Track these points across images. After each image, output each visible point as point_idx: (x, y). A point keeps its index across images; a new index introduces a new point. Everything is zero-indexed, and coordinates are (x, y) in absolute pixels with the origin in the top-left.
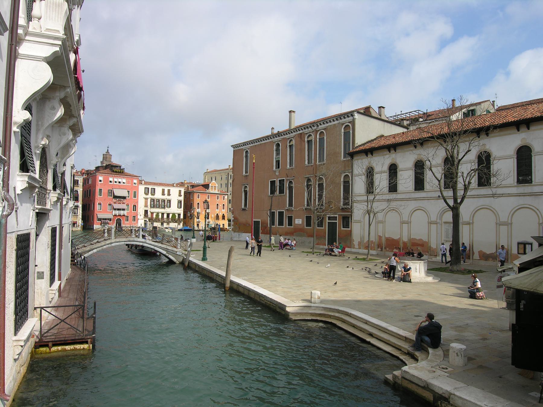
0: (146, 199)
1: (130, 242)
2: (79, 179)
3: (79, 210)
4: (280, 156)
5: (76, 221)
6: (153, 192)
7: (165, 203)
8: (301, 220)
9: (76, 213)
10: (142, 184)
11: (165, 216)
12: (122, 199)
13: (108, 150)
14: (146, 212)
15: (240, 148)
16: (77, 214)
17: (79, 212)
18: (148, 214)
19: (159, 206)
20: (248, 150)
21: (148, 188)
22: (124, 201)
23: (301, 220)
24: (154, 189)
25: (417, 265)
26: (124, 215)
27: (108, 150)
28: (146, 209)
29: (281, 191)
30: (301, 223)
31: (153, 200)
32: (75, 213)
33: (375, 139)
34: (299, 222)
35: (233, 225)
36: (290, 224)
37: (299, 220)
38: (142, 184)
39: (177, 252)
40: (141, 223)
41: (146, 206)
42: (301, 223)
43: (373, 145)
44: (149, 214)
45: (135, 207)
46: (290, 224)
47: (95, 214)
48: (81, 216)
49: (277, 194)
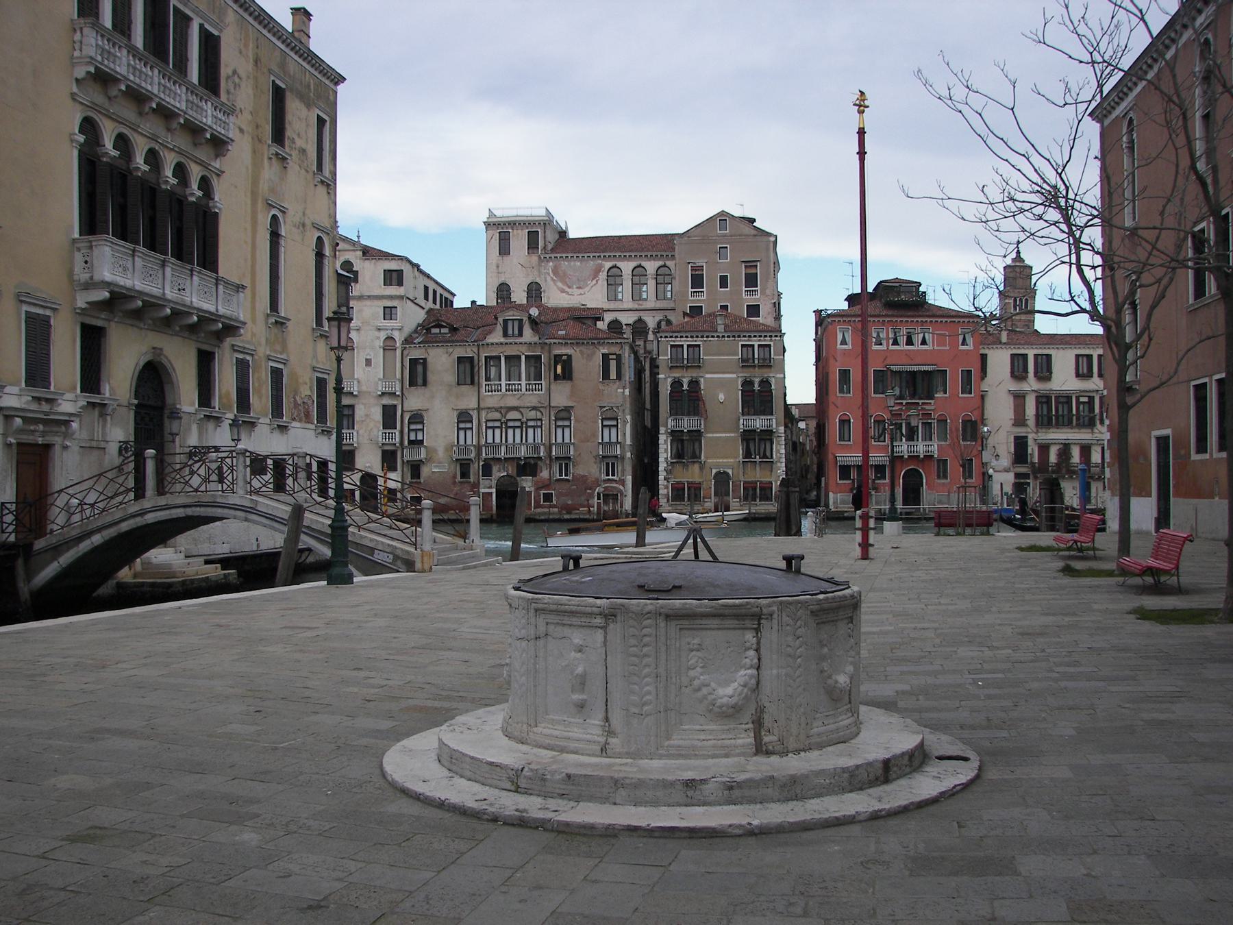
0: (1019, 398)
1: (202, 509)
2: (772, 343)
3: (778, 443)
5: (768, 480)
6: (1045, 368)
7: (1050, 409)
9: (768, 454)
10: (1001, 343)
11: (1076, 453)
12: (921, 402)
14: (1021, 444)
15: (1114, 116)
16: (772, 458)
17: (778, 451)
18: (1030, 451)
19: (1050, 419)
21: (1025, 356)
22: (927, 407)
24: (1049, 357)
25: (577, 638)
26: (929, 457)
27: (1018, 252)
28: (1021, 431)
31: (1043, 400)
32: (765, 456)
38: (1001, 343)
40: (1003, 480)
41: (1020, 420)
44: (1033, 449)
45: (972, 429)
47: (830, 457)
48: (784, 465)
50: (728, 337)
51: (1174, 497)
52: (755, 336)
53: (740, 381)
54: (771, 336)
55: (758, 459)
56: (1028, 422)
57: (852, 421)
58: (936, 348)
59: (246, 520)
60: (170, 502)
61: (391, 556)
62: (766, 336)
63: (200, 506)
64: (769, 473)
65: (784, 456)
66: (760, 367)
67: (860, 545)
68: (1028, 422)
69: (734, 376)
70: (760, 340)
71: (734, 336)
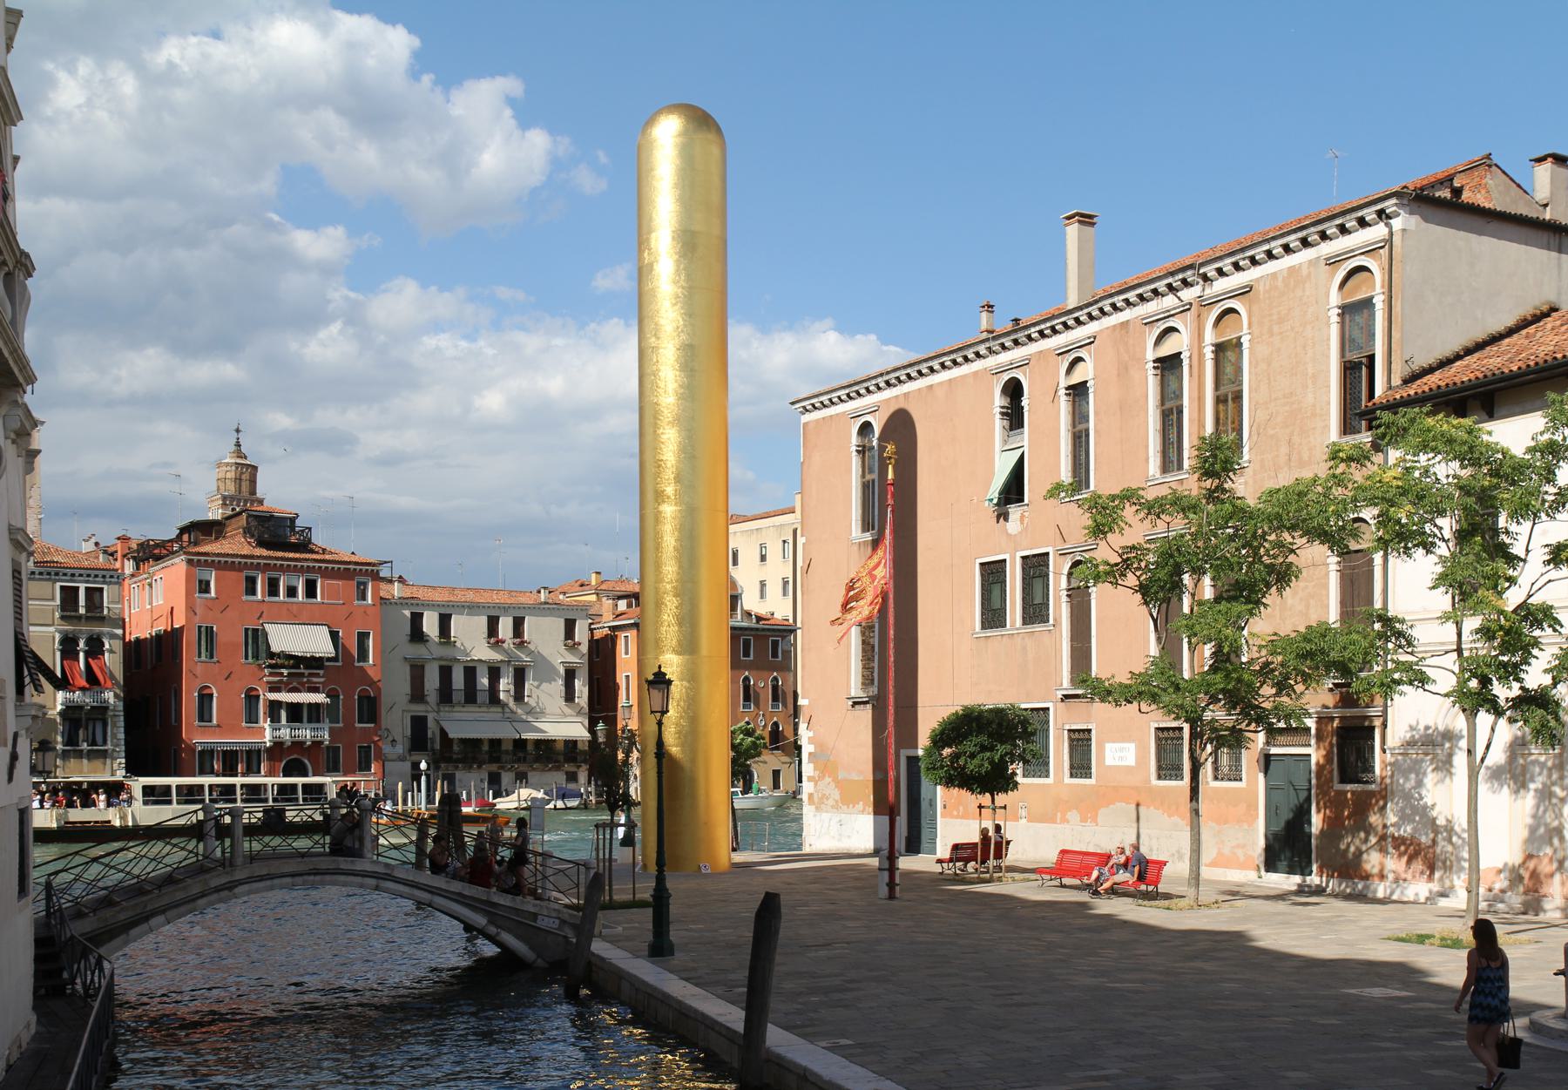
4: (1026, 443)
8: (1132, 746)
13: (238, 445)
14: (419, 724)
18: (430, 735)
20: (869, 418)
22: (315, 680)
23: (1132, 746)
28: (419, 709)
29: (1035, 612)
30: (1130, 760)
33: (1511, 332)
34: (1121, 758)
35: (810, 779)
36: (1081, 766)
37: (1122, 750)
39: (535, 916)
41: (418, 695)
42: (1130, 760)
43: (1495, 361)
46: (1081, 766)
49: (1013, 624)
50: (41, 574)
51: (942, 816)
52: (81, 575)
53: (58, 637)
54: (104, 577)
55: (85, 746)
56: (428, 699)
57: (215, 695)
58: (326, 601)
59: (377, 888)
60: (273, 871)
61: (557, 921)
62: (96, 576)
63: (315, 874)
64: (101, 766)
65: (123, 742)
66: (88, 618)
67: (887, 885)
68: (429, 699)
69: (52, 629)
70: (87, 582)
71: (49, 574)
